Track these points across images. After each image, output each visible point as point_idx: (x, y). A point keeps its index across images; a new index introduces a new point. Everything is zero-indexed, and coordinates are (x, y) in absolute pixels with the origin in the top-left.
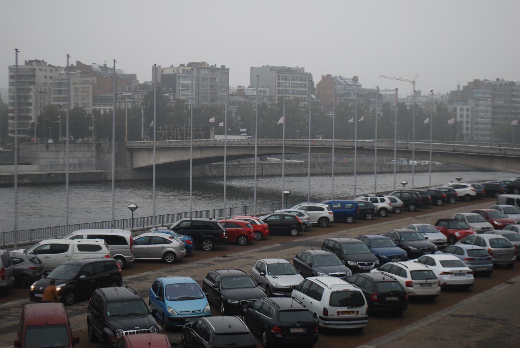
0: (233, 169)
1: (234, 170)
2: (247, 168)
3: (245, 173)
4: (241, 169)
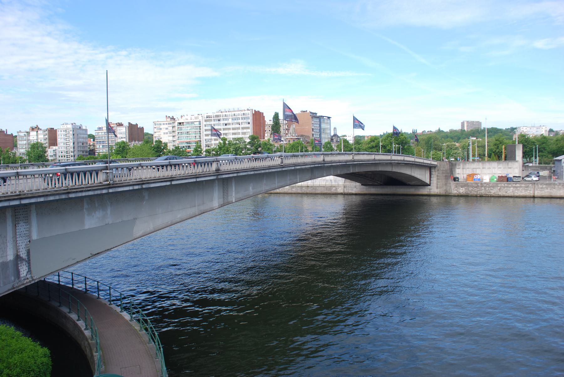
0: (489, 188)
1: (489, 189)
2: (510, 187)
3: (506, 192)
4: (500, 188)
